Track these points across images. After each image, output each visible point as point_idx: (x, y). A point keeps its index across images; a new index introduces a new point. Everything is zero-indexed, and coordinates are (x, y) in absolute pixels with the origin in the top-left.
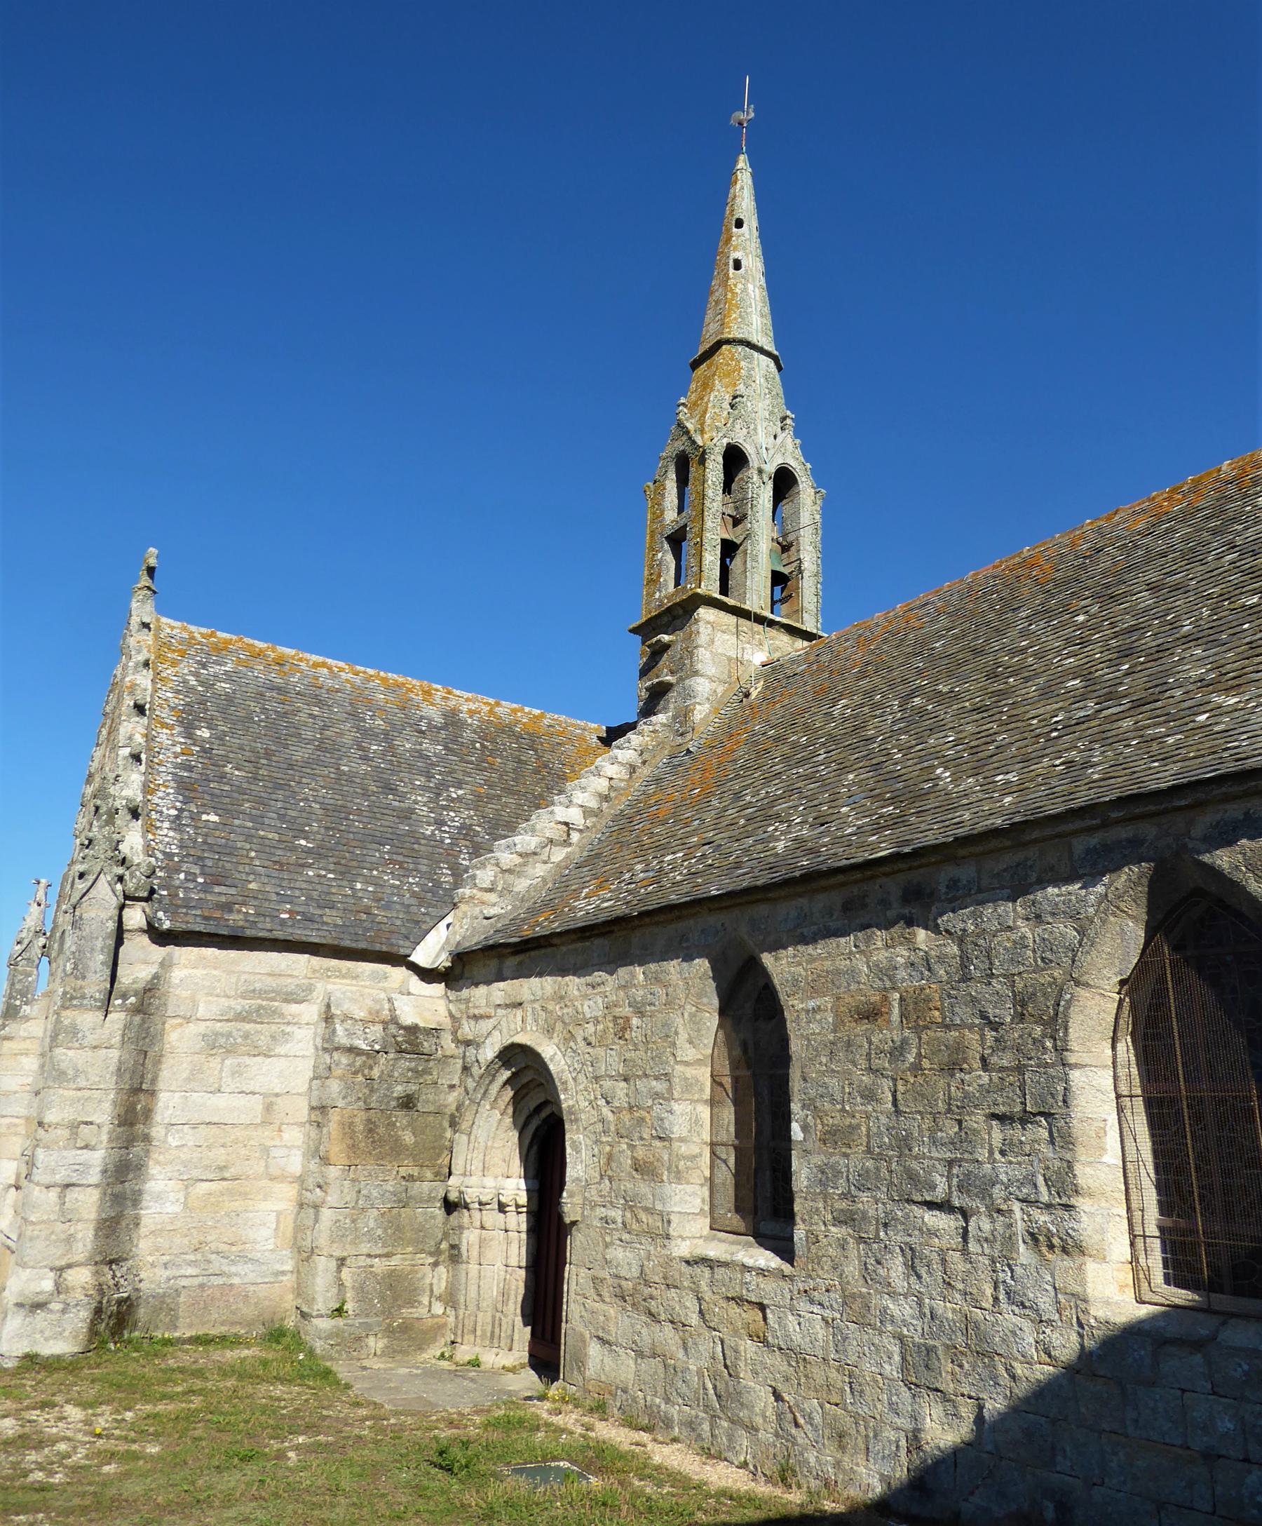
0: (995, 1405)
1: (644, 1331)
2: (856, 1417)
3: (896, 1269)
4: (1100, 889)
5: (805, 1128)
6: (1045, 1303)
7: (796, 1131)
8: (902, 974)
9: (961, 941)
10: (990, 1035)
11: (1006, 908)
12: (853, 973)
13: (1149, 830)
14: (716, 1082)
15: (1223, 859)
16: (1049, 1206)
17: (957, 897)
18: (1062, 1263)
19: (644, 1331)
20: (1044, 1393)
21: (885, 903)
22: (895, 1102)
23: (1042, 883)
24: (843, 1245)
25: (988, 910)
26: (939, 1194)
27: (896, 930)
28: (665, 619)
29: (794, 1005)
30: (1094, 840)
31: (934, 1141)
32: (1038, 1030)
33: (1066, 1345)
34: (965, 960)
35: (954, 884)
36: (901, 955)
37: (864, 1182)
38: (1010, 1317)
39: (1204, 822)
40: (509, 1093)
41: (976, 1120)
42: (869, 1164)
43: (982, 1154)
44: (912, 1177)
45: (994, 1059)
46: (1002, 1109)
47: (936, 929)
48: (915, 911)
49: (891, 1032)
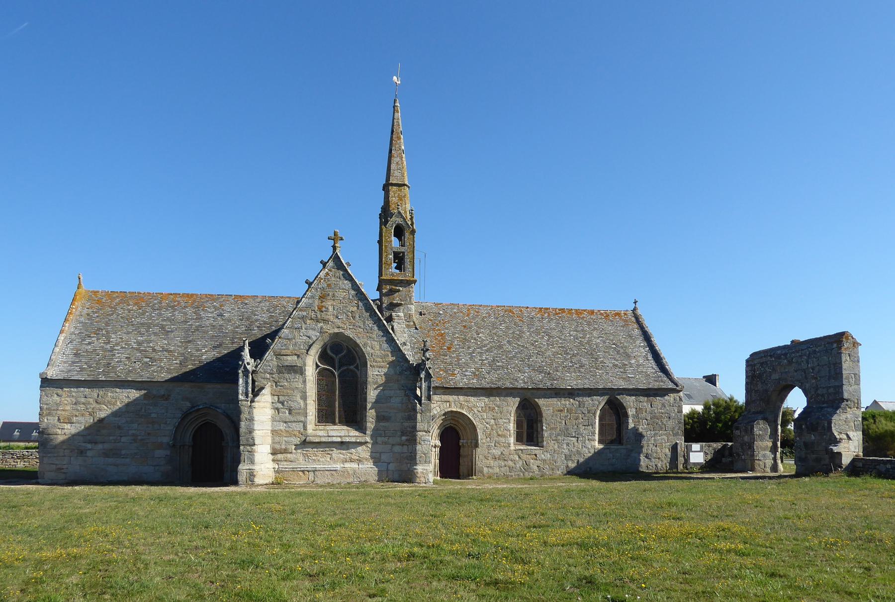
0: (581, 460)
1: (502, 463)
2: (556, 466)
3: (565, 446)
4: (602, 398)
5: (546, 427)
6: (590, 447)
7: (544, 428)
8: (567, 405)
9: (579, 402)
10: (583, 415)
11: (587, 398)
12: (557, 404)
13: (609, 392)
14: (514, 420)
15: (618, 397)
16: (591, 436)
17: (578, 396)
18: (592, 442)
19: (502, 463)
20: (590, 458)
21: (564, 394)
22: (565, 423)
23: (593, 396)
24: (555, 444)
25: (585, 398)
26: (574, 435)
27: (567, 399)
28: (398, 281)
29: (543, 409)
30: (602, 392)
31: (573, 429)
32: (591, 415)
33: (592, 451)
34: (580, 405)
35: (578, 394)
36: (567, 403)
37: (558, 435)
38: (584, 449)
39: (616, 392)
40: (442, 422)
41: (581, 426)
42: (560, 432)
43: (581, 430)
44: (569, 434)
45: (584, 418)
46: (585, 424)
47: (574, 399)
48: (570, 396)
49: (565, 413)
